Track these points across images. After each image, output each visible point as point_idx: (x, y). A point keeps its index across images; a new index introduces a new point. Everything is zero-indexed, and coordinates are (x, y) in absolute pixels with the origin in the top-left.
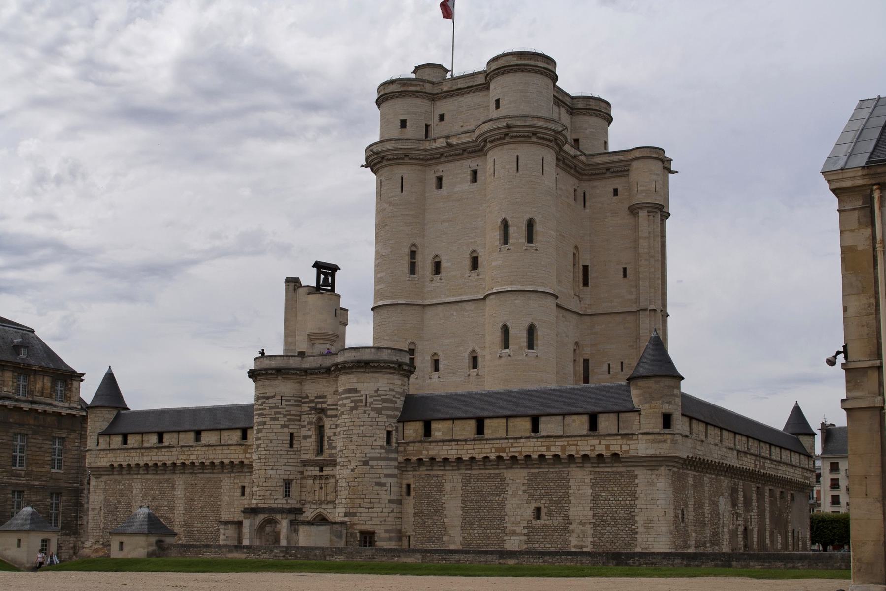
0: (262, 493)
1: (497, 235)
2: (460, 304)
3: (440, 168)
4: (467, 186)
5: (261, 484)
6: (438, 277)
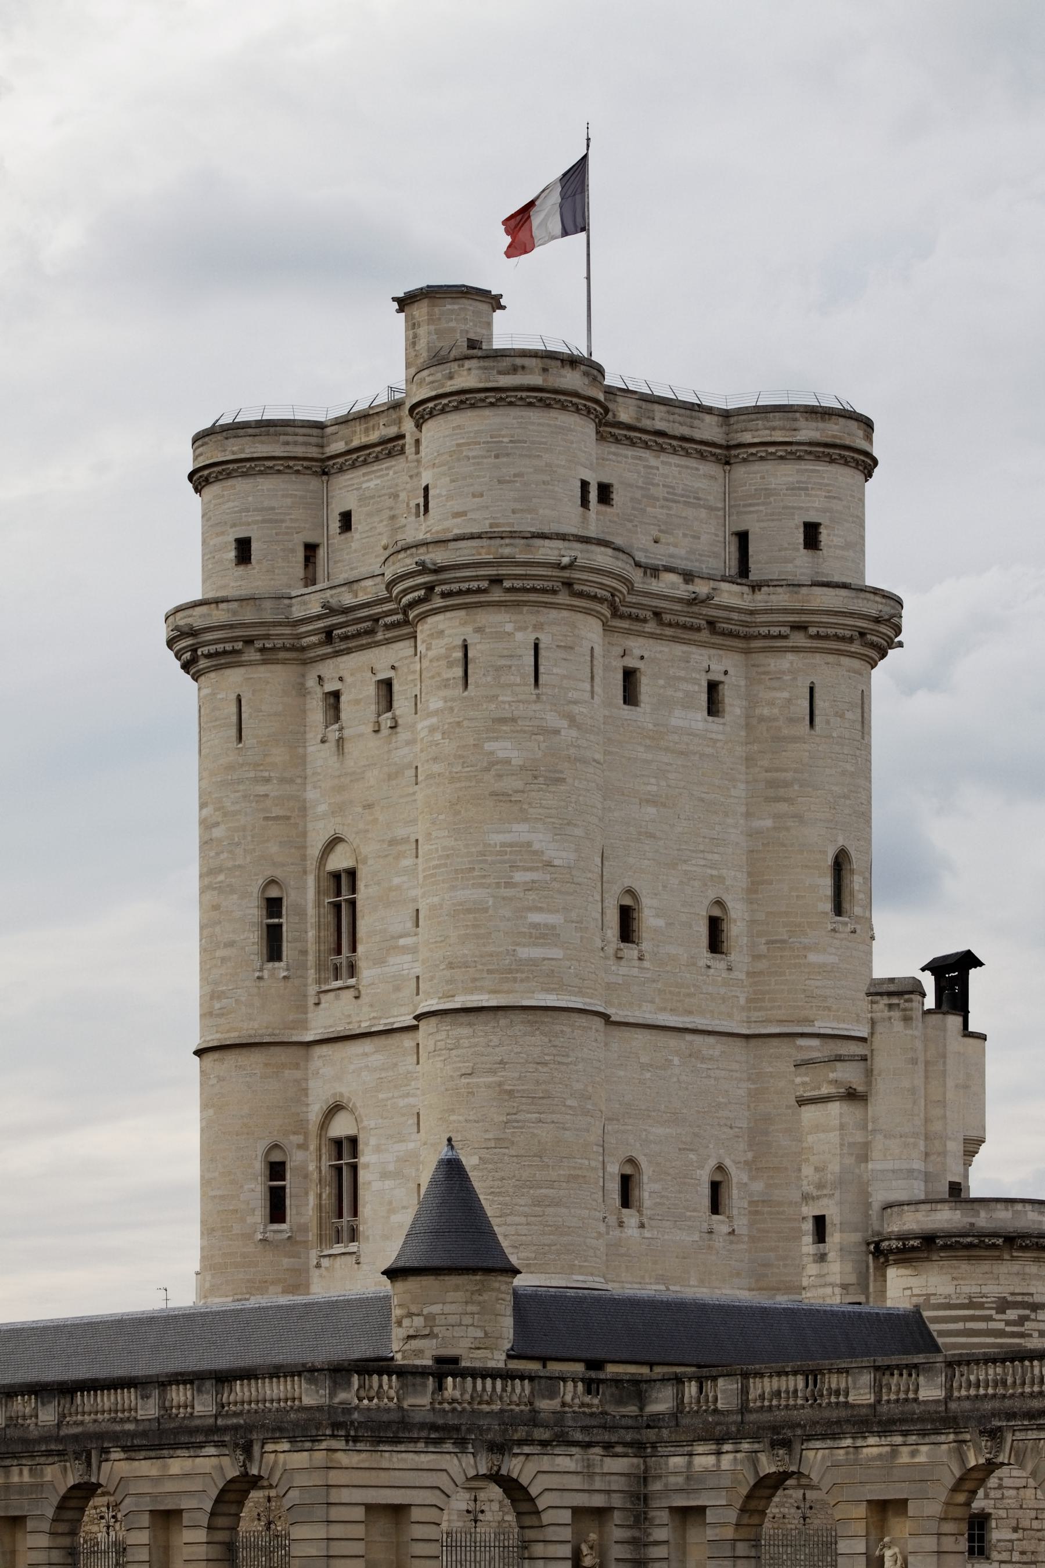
0: (1026, 1545)
1: (826, 883)
2: (689, 1037)
3: (638, 646)
4: (698, 718)
5: (1025, 1523)
6: (630, 951)
